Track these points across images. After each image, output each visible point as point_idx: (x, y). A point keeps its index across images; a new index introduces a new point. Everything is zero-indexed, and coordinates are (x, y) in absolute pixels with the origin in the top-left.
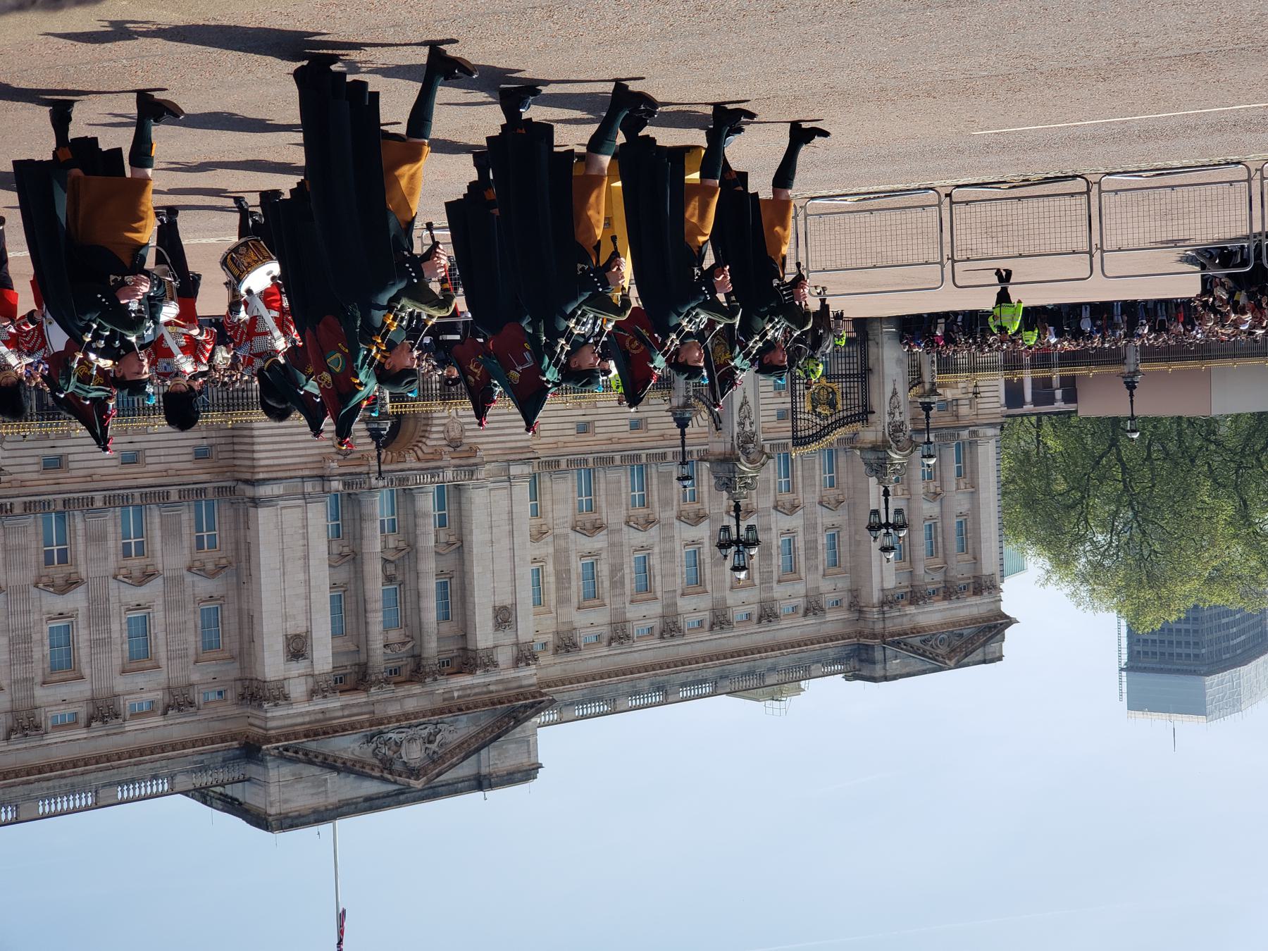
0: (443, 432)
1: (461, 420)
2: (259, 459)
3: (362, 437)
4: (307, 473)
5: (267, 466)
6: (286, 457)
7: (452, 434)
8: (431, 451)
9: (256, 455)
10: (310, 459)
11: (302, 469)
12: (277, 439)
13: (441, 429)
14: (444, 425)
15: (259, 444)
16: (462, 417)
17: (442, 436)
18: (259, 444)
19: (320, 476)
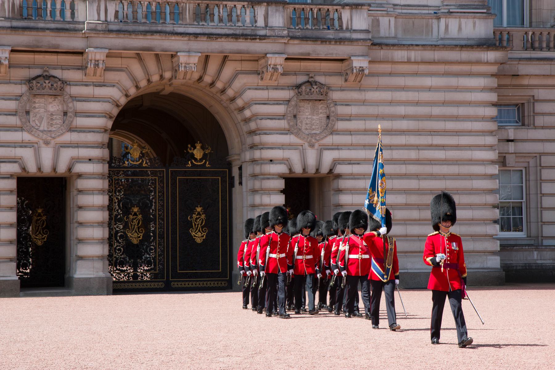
0: (77, 114)
1: (27, 137)
2: (484, 89)
3: (272, 117)
4: (400, 54)
5: (470, 75)
6: (430, 89)
7: (54, 106)
8: (111, 76)
9: (493, 97)
10: (384, 81)
11: (409, 62)
12: (450, 125)
13: (81, 122)
14: (71, 130)
15: (483, 119)
16: (23, 145)
17: (80, 106)
18: (483, 119)
19: (380, 45)
